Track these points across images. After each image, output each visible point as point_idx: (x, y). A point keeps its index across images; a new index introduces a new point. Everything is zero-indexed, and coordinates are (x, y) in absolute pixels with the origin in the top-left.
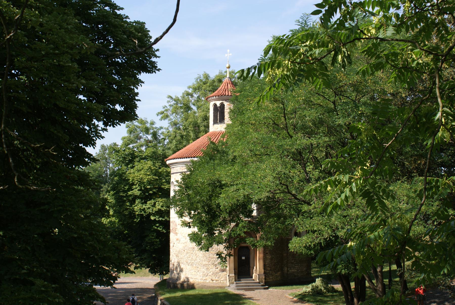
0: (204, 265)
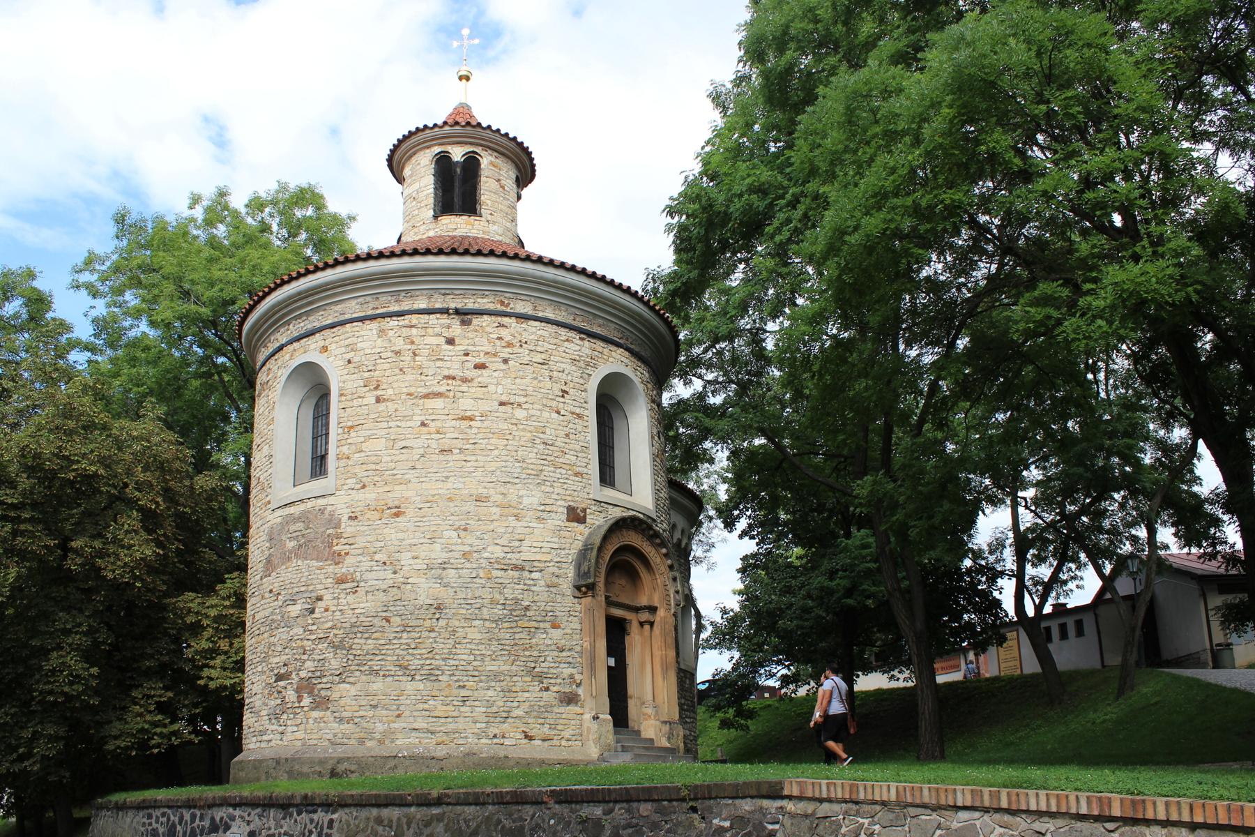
0: (496, 676)
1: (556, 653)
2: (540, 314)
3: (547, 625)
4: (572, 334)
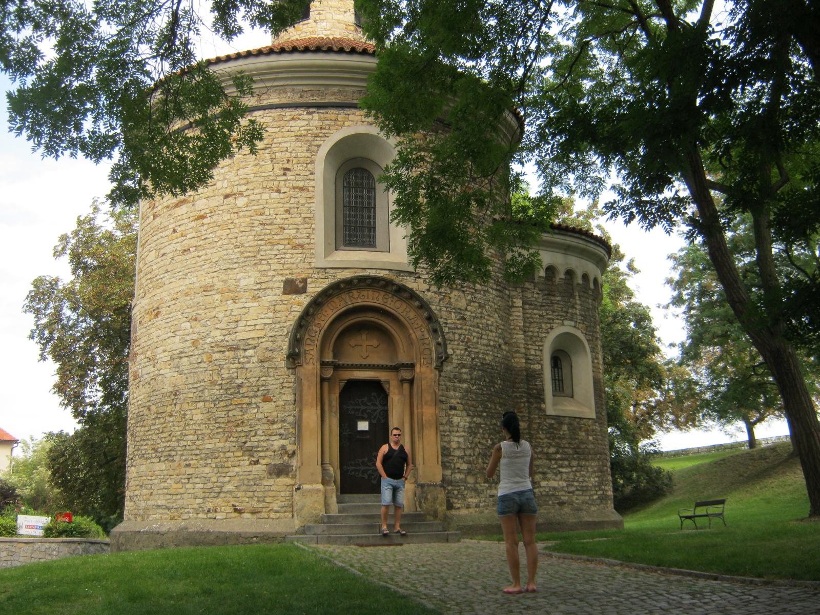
0: (212, 454)
1: (266, 426)
2: (265, 103)
3: (259, 400)
4: (299, 111)
